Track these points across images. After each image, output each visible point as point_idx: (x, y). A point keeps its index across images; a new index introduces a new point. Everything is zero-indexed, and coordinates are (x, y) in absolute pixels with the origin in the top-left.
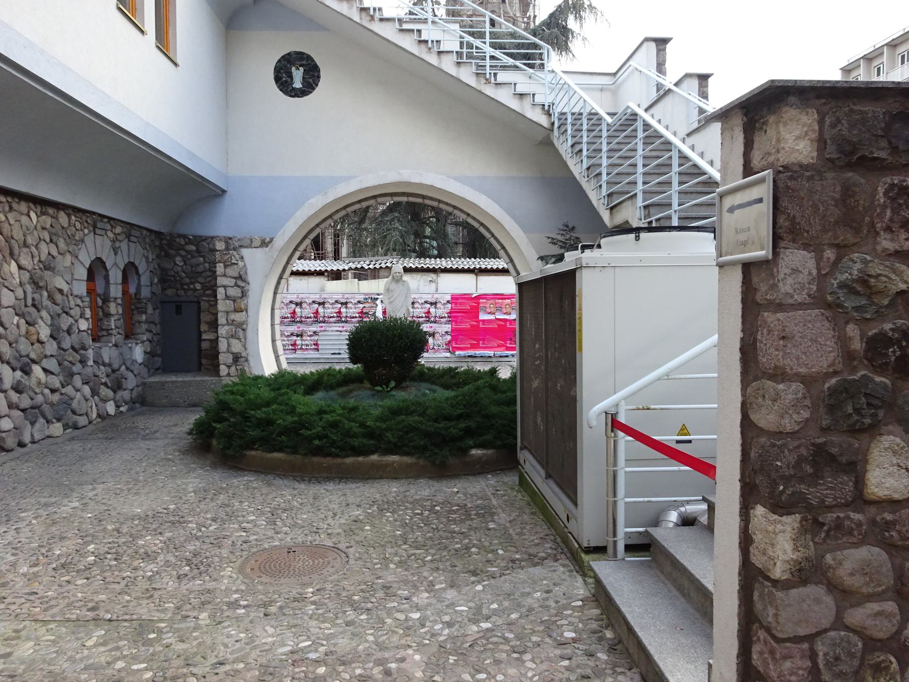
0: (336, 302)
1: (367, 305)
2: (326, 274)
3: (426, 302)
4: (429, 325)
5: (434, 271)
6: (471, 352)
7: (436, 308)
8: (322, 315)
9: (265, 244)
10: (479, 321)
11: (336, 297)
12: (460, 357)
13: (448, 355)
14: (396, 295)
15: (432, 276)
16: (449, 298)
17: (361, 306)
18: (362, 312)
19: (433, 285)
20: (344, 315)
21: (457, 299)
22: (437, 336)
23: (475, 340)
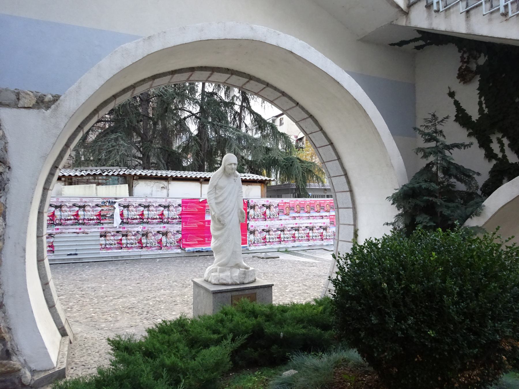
0: (74, 205)
1: (105, 208)
2: (63, 179)
3: (160, 206)
4: (162, 225)
5: (166, 179)
6: (199, 248)
7: (168, 210)
8: (58, 217)
9: (42, 103)
10: (204, 222)
11: (74, 201)
12: (189, 252)
13: (179, 251)
14: (225, 195)
15: (164, 183)
16: (180, 202)
17: (99, 209)
18: (99, 215)
19: (165, 191)
20: (82, 217)
21: (187, 203)
22: (169, 235)
23: (201, 237)
